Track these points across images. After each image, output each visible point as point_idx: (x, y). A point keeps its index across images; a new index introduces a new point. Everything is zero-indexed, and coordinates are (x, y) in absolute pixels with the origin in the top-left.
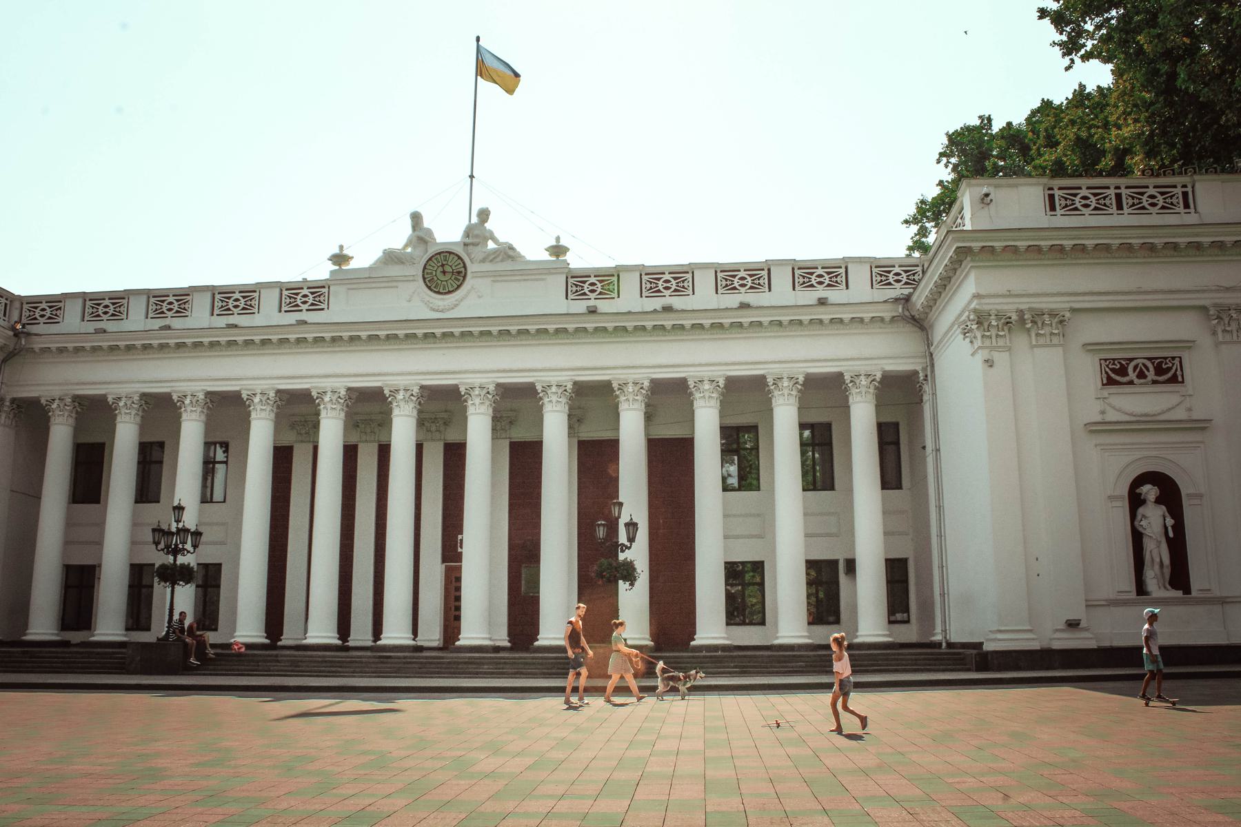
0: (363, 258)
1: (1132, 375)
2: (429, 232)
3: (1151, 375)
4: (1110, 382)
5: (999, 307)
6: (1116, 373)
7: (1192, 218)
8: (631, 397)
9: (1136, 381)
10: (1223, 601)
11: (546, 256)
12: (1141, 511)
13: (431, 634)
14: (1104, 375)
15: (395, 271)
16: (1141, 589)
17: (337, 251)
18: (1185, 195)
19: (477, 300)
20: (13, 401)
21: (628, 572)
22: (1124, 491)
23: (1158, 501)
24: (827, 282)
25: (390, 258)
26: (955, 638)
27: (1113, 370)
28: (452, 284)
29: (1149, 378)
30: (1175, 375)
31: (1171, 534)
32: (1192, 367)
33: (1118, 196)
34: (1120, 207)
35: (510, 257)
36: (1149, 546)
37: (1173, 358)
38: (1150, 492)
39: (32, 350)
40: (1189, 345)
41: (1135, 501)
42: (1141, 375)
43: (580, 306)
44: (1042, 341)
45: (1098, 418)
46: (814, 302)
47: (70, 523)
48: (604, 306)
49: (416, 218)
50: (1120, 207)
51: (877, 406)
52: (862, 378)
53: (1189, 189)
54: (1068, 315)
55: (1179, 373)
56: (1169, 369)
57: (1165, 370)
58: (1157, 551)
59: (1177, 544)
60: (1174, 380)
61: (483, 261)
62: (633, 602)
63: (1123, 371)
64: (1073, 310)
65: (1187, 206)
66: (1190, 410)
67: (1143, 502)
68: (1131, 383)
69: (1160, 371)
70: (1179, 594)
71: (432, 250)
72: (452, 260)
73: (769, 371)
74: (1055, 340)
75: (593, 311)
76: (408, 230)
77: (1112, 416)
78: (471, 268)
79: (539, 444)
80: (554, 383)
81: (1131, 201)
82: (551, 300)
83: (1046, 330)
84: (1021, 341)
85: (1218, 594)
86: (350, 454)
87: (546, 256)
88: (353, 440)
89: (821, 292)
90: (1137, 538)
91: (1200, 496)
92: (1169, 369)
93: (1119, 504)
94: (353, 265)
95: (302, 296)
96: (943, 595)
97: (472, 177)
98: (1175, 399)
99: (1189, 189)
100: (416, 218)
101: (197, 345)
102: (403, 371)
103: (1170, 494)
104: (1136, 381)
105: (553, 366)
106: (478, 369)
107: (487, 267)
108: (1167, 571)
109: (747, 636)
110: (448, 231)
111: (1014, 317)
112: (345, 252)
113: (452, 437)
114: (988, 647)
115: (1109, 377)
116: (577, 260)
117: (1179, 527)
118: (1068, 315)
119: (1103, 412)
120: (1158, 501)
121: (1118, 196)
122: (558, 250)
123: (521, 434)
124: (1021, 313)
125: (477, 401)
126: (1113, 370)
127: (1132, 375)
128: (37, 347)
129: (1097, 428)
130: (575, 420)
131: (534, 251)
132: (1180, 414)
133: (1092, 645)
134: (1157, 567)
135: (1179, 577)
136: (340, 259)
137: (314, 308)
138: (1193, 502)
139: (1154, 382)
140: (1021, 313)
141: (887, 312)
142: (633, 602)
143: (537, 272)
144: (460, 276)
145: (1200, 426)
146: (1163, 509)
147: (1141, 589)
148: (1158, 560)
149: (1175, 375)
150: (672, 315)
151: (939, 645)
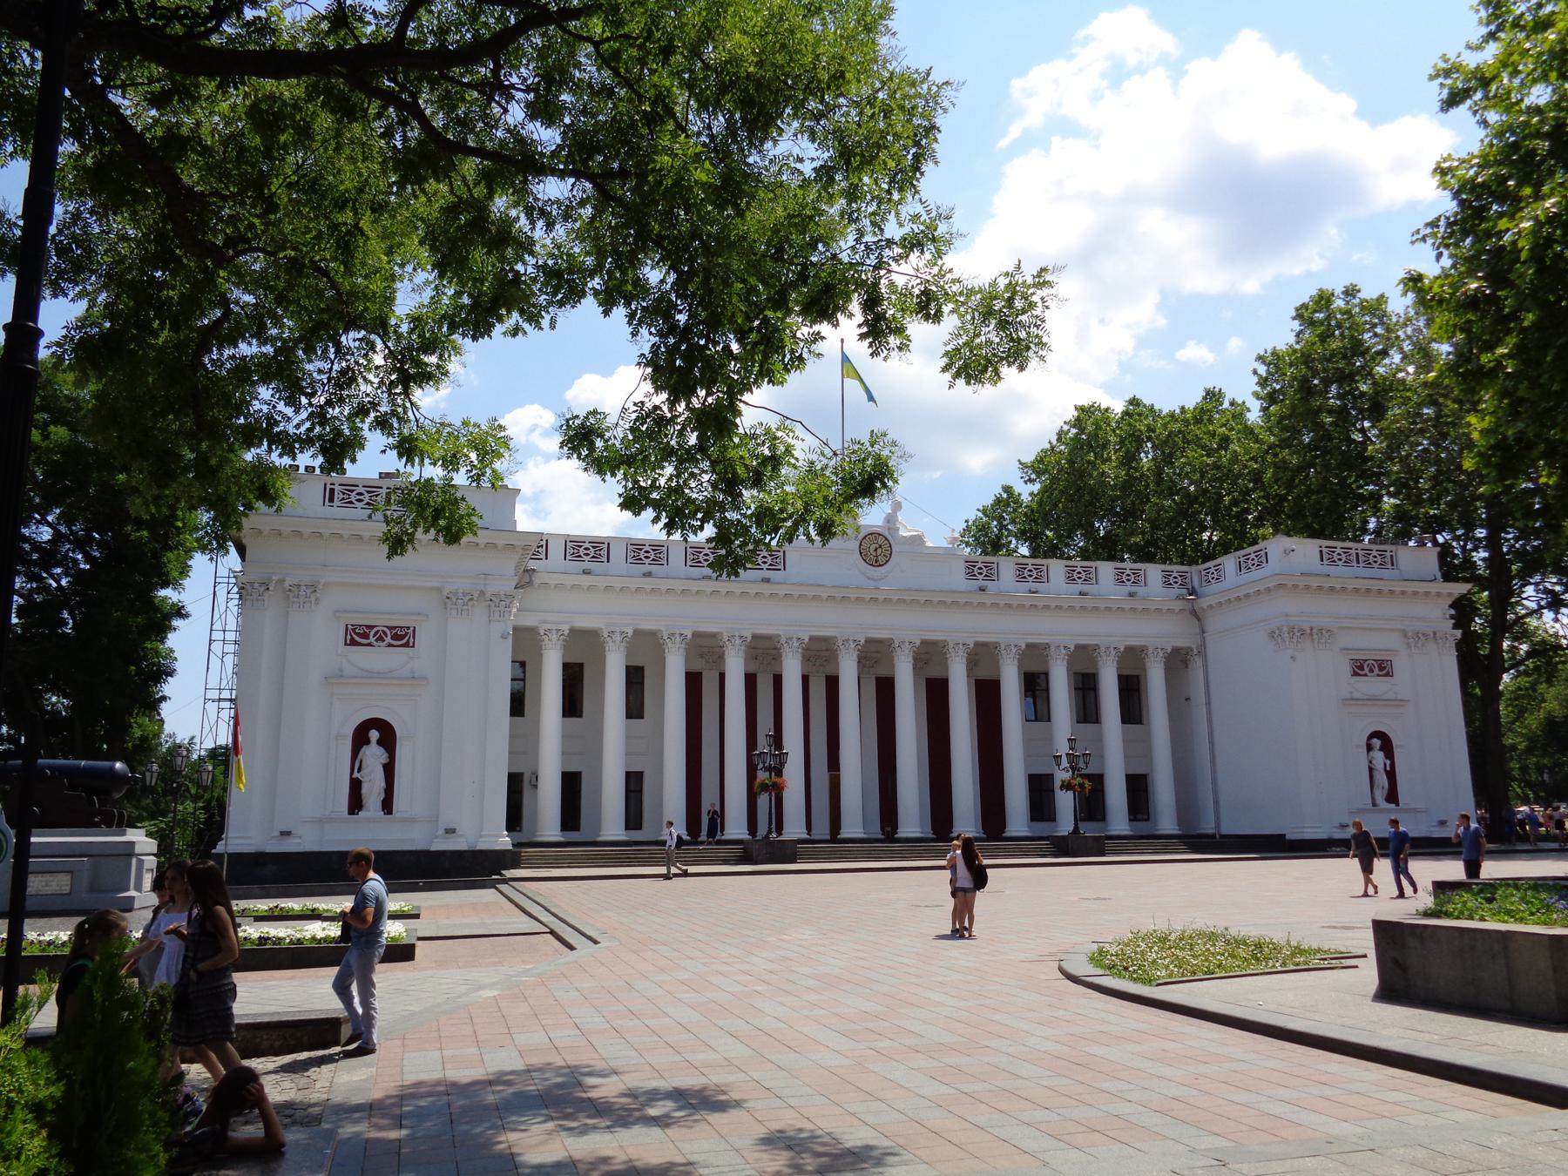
1: (1367, 670)
3: (1376, 671)
4: (1355, 674)
6: (1359, 669)
10: (1415, 811)
11: (945, 545)
13: (822, 829)
16: (1374, 804)
21: (1067, 786)
22: (1364, 742)
26: (1225, 831)
32: (1398, 667)
38: (1377, 742)
41: (1369, 748)
43: (975, 584)
47: (566, 737)
57: (1384, 668)
59: (1391, 774)
60: (1387, 675)
63: (1361, 668)
69: (1381, 669)
72: (881, 540)
75: (982, 589)
77: (1356, 695)
86: (751, 681)
88: (752, 670)
96: (1216, 803)
102: (851, 625)
106: (906, 628)
109: (1142, 828)
113: (831, 672)
114: (1288, 837)
117: (1393, 765)
127: (1367, 670)
129: (1350, 701)
132: (1390, 695)
135: (1392, 797)
141: (1177, 609)
147: (1374, 804)
151: (1213, 836)
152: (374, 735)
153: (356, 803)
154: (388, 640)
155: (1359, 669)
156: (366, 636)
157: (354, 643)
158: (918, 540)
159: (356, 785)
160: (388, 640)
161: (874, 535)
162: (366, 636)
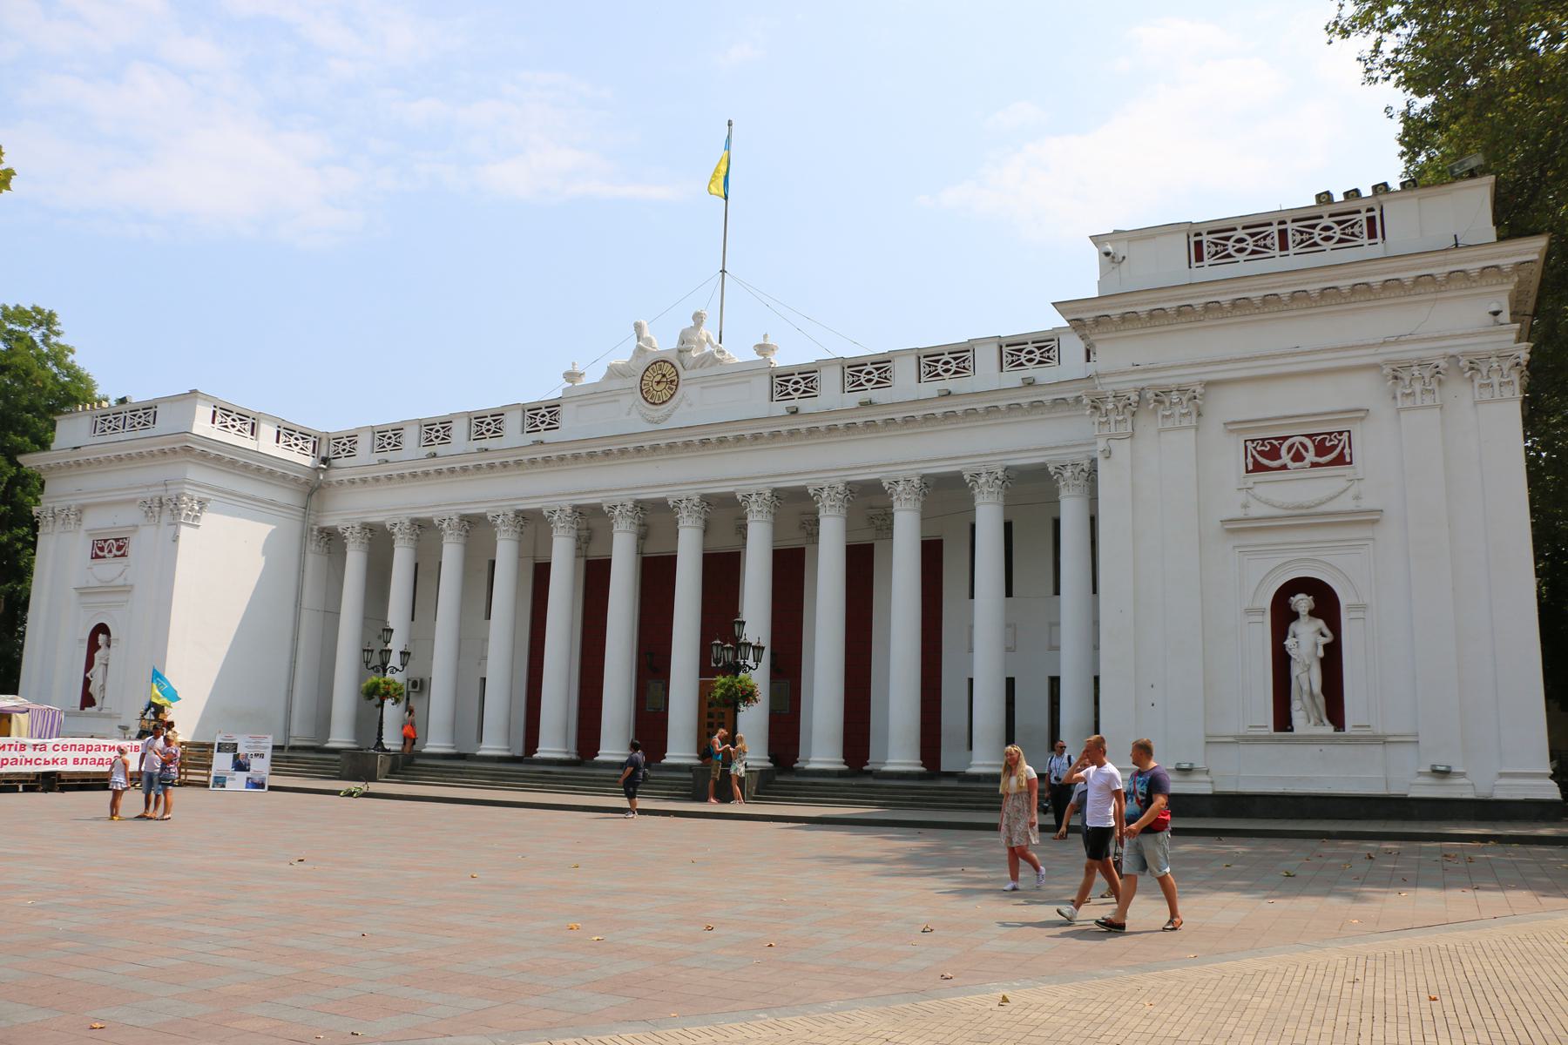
0: (594, 375)
1: (1286, 458)
2: (649, 342)
3: (1310, 456)
4: (1259, 468)
5: (1115, 387)
7: (1378, 250)
8: (1070, 482)
9: (1291, 464)
11: (754, 356)
12: (1293, 627)
14: (1250, 459)
15: (616, 384)
16: (1283, 720)
17: (570, 368)
18: (1371, 220)
19: (694, 407)
20: (322, 530)
22: (1267, 603)
23: (1313, 613)
24: (1038, 358)
25: (614, 372)
27: (1261, 453)
28: (665, 395)
29: (1307, 462)
30: (1342, 454)
31: (1321, 653)
32: (1364, 445)
33: (1283, 233)
34: (1284, 246)
35: (718, 361)
36: (1296, 670)
37: (1341, 433)
38: (1302, 602)
39: (329, 484)
40: (1361, 414)
41: (1282, 616)
42: (1298, 457)
43: (781, 408)
44: (1169, 424)
45: (1239, 513)
46: (1019, 383)
48: (806, 405)
49: (638, 327)
50: (1284, 246)
51: (847, 521)
52: (1069, 469)
53: (1377, 214)
54: (1199, 390)
55: (1347, 451)
56: (1334, 447)
57: (1330, 450)
58: (1307, 676)
60: (1340, 460)
61: (694, 367)
62: (753, 721)
63: (1274, 453)
64: (1208, 384)
65: (1372, 235)
66: (1357, 498)
67: (1295, 616)
68: (1284, 467)
69: (1321, 450)
70: (1328, 729)
71: (650, 360)
72: (667, 368)
73: (965, 467)
74: (1185, 423)
76: (633, 343)
77: (1257, 510)
78: (683, 375)
79: (674, 558)
80: (753, 492)
81: (1298, 238)
82: (757, 402)
83: (1178, 410)
84: (1148, 425)
85: (1380, 732)
87: (754, 356)
89: (1031, 371)
90: (1282, 663)
91: (1363, 607)
92: (1334, 447)
93: (1259, 618)
94: (585, 381)
95: (543, 415)
97: (723, 271)
98: (1341, 484)
99: (1377, 214)
100: (638, 327)
101: (722, 441)
103: (1326, 604)
104: (1291, 464)
105: (751, 473)
106: (681, 479)
107: (697, 373)
108: (1321, 700)
110: (664, 342)
111: (1134, 397)
112: (769, 342)
115: (1256, 461)
116: (780, 360)
118: (1199, 390)
119: (1245, 506)
120: (1313, 613)
121: (1283, 233)
122: (763, 349)
123: (595, 553)
124: (1141, 392)
125: (685, 514)
126: (1261, 453)
127: (1286, 458)
128: (334, 480)
129: (1237, 527)
130: (643, 537)
131: (739, 352)
133: (1206, 789)
134: (1306, 698)
135: (1334, 711)
136: (571, 376)
137: (552, 426)
138: (1353, 615)
139: (1314, 465)
140: (1141, 392)
142: (753, 721)
143: (744, 373)
144: (674, 384)
145: (1369, 519)
146: (1320, 623)
147: (1283, 720)
148: (1306, 687)
149: (1342, 454)
150: (542, 448)
152: (102, 638)
153: (88, 700)
154: (114, 551)
155: (1266, 455)
156: (102, 549)
157: (97, 557)
158: (709, 360)
159: (87, 682)
160: (114, 551)
161: (661, 362)
162: (102, 549)
